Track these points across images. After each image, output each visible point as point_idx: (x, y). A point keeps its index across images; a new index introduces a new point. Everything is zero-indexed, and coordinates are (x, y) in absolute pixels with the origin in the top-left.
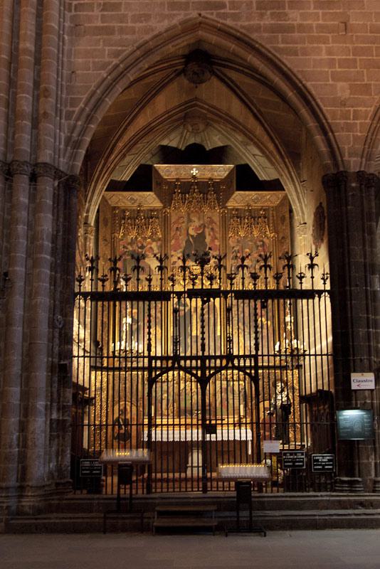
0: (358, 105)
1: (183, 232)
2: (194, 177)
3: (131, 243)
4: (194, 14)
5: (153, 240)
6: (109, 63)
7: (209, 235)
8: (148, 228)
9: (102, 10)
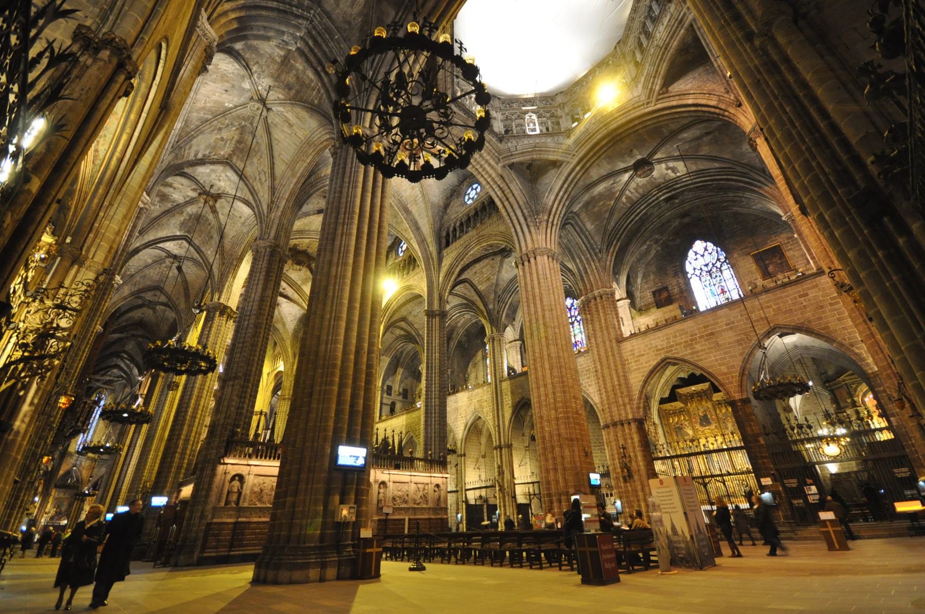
4: (663, 356)
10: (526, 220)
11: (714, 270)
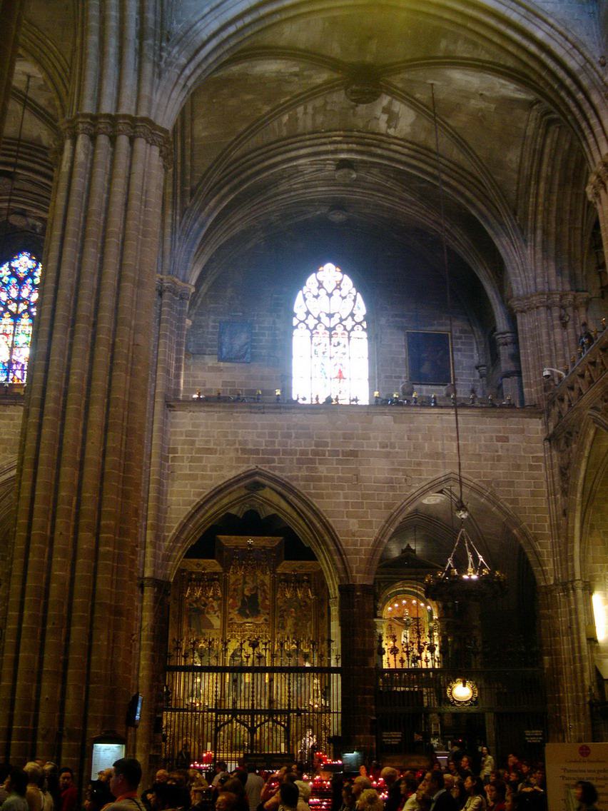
0: (363, 536)
2: (250, 545)
4: (253, 467)
5: (214, 600)
6: (194, 501)
8: (210, 589)
9: (190, 462)
10: (141, 35)
11: (339, 329)
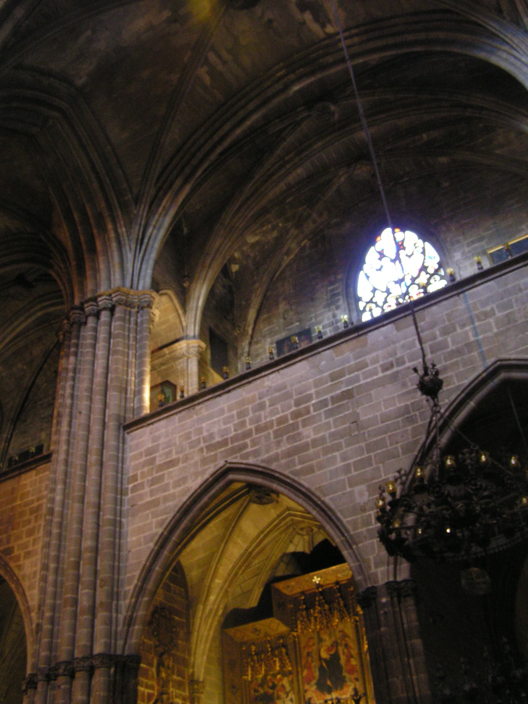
1: (315, 657)
2: (319, 586)
3: (262, 685)
6: (156, 534)
7: (344, 653)
